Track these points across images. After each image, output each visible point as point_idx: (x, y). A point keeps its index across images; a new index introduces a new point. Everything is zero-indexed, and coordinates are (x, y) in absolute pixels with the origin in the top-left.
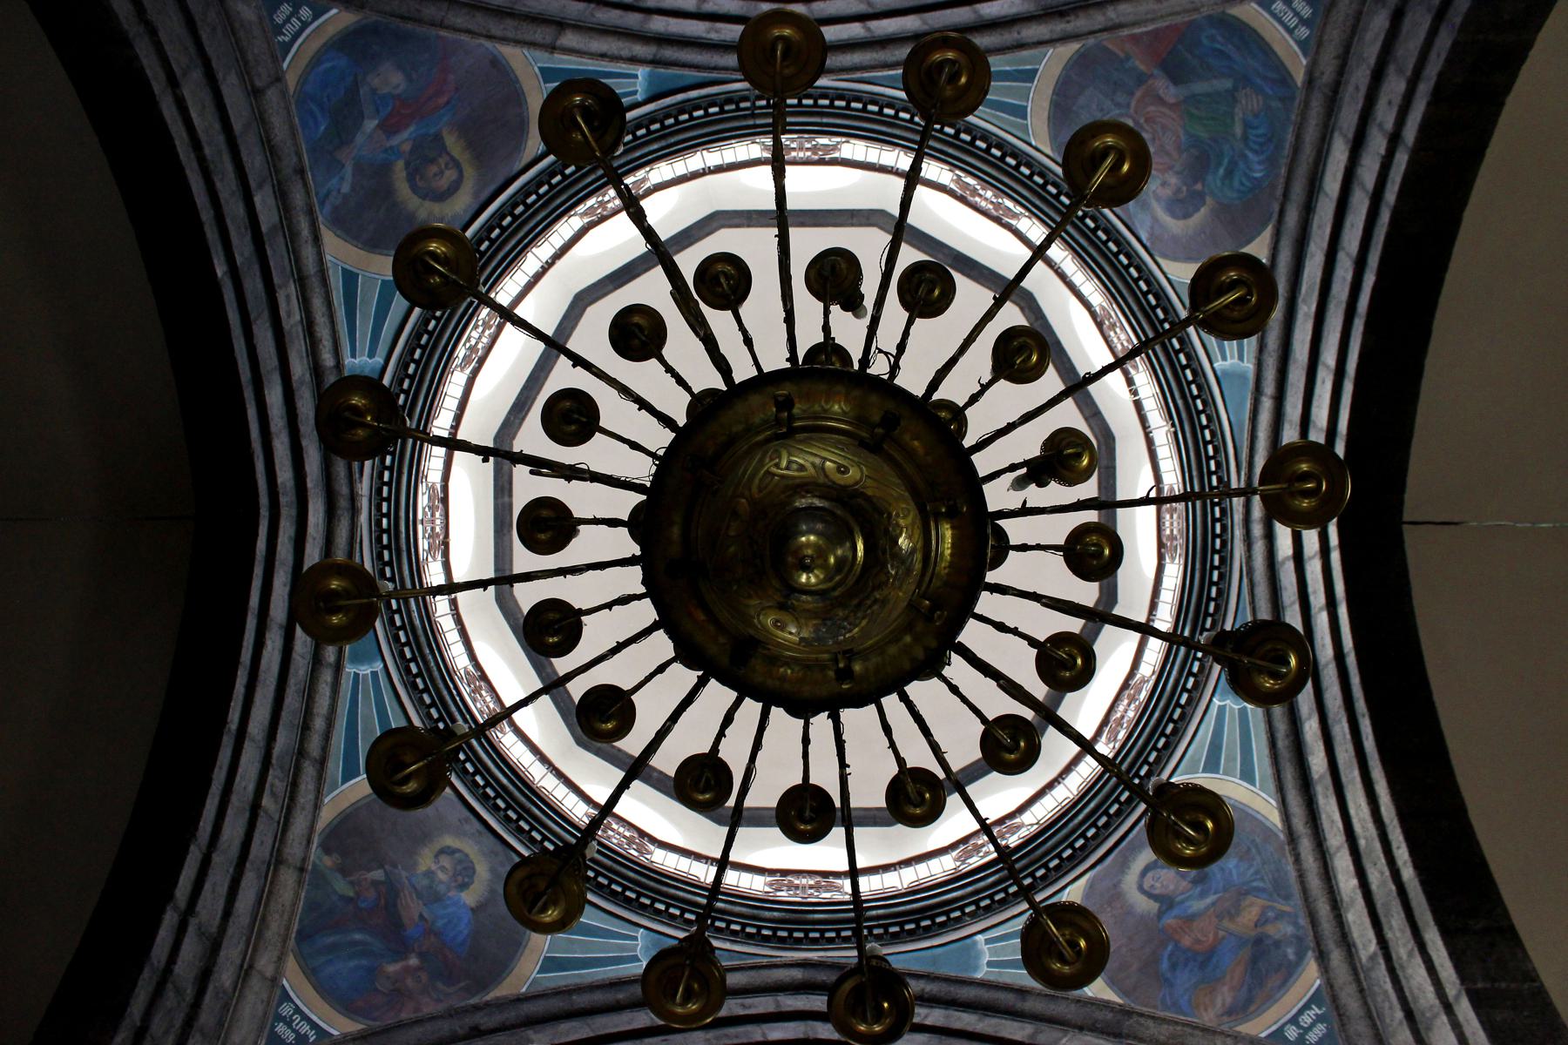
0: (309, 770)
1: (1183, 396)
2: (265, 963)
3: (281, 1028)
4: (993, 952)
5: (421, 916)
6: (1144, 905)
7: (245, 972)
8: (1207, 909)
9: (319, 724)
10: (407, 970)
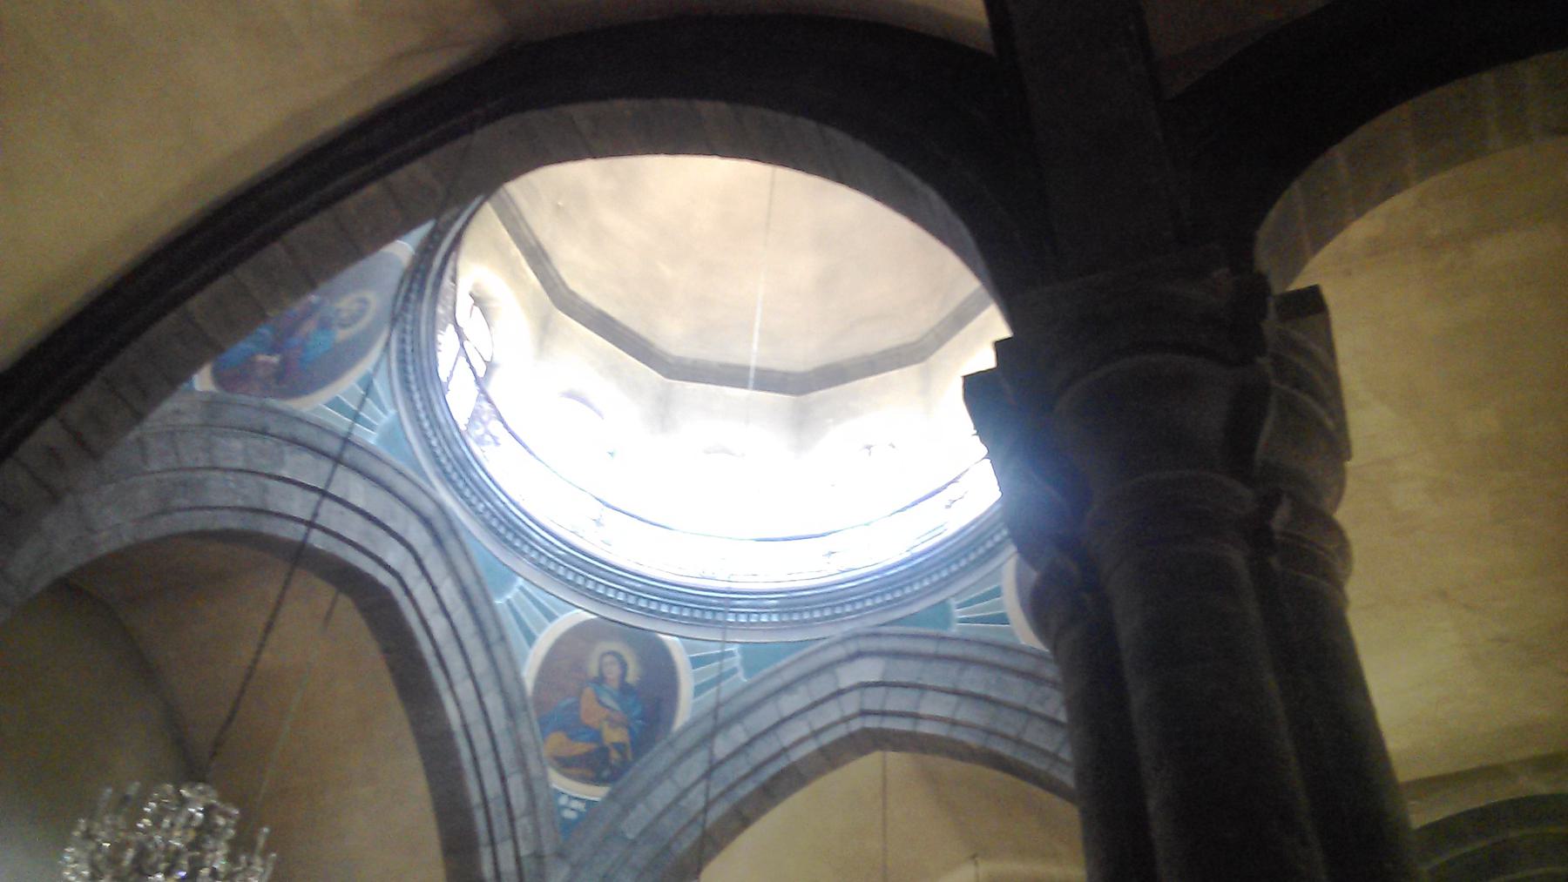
1: (930, 568)
4: (517, 597)
8: (608, 707)
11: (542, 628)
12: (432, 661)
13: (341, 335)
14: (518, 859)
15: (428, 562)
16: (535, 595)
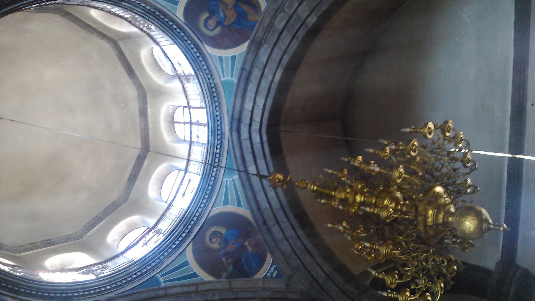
0: (201, 288)
2: (260, 285)
3: (274, 275)
4: (227, 76)
5: (233, 244)
6: (218, 30)
7: (264, 289)
9: (186, 289)
10: (250, 244)
11: (226, 58)
12: (271, 95)
13: (223, 231)
14: (300, 4)
15: (248, 122)
16: (220, 66)
